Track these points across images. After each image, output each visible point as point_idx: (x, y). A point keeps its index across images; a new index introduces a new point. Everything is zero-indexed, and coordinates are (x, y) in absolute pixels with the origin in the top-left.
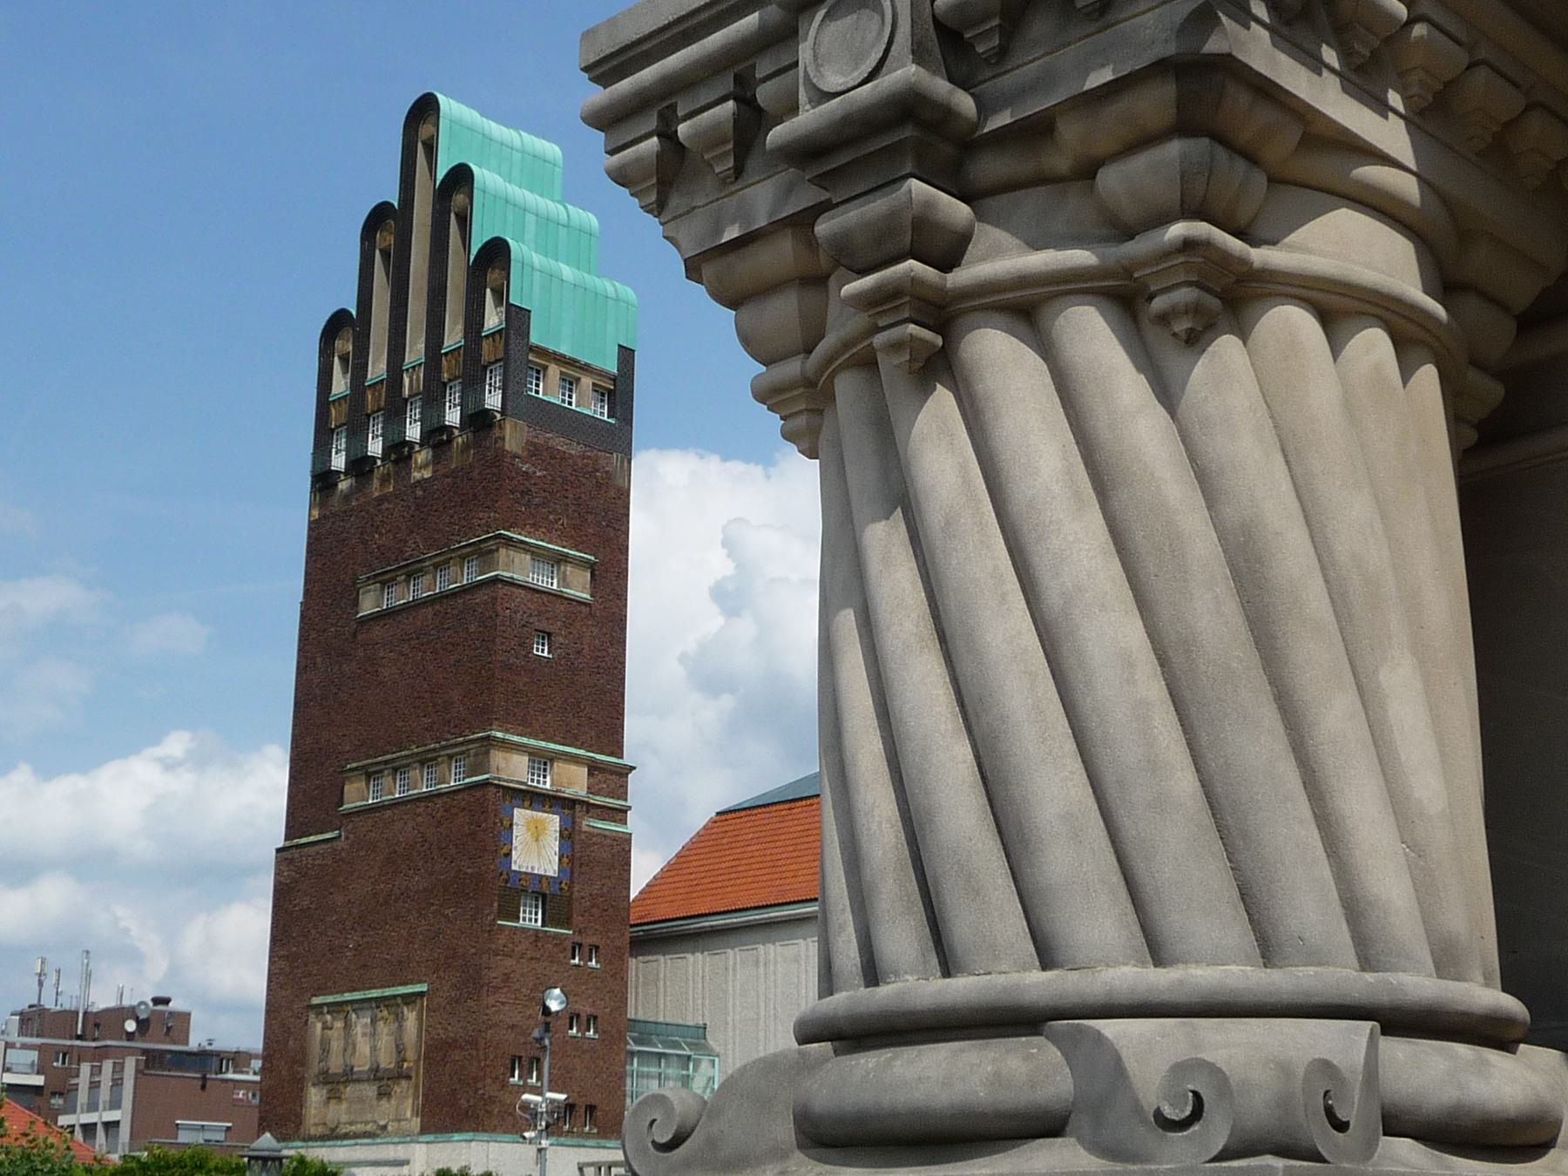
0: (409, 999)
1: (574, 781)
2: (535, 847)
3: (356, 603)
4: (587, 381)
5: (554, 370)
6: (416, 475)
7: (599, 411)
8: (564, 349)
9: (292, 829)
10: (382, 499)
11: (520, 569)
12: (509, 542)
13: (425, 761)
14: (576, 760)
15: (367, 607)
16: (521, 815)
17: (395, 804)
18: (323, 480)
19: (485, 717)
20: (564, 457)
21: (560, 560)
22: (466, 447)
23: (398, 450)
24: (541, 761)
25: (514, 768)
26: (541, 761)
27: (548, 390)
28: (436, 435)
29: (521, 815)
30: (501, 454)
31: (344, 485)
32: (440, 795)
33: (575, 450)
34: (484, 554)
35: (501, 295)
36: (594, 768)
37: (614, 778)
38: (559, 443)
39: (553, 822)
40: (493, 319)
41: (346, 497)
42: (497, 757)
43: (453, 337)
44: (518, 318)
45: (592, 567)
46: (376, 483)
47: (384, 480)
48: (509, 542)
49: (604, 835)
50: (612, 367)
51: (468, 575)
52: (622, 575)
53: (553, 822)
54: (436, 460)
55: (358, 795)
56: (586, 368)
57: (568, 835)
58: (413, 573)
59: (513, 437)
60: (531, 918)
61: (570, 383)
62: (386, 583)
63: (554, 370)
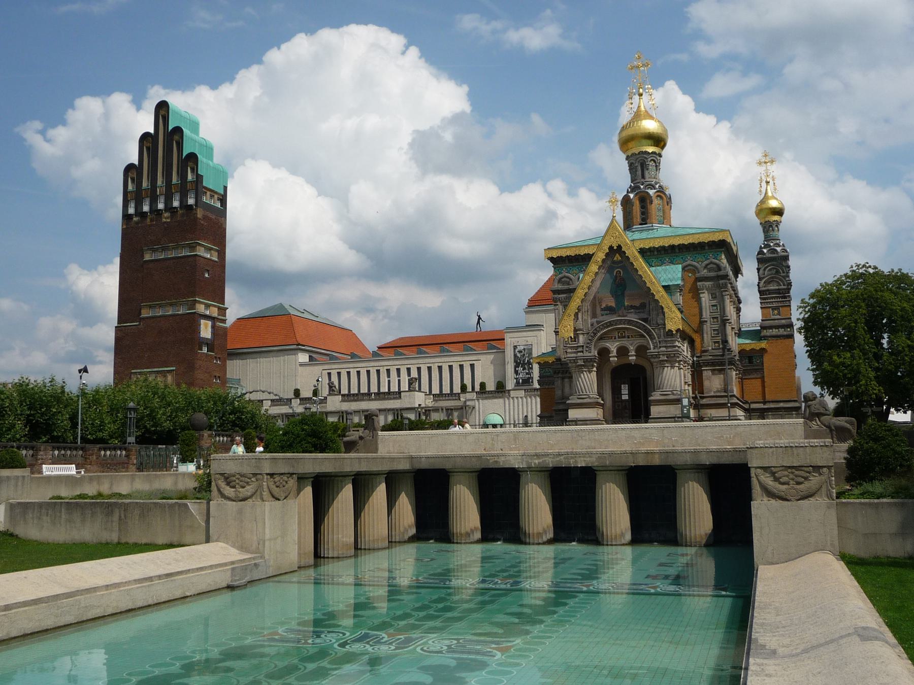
0: (169, 371)
1: (214, 312)
2: (206, 331)
3: (143, 256)
4: (216, 196)
5: (208, 193)
6: (164, 220)
7: (218, 205)
8: (211, 187)
9: (120, 319)
10: (151, 225)
11: (201, 252)
12: (200, 245)
13: (171, 305)
14: (215, 306)
15: (147, 257)
16: (203, 321)
17: (160, 317)
18: (126, 217)
19: (193, 294)
20: (211, 219)
21: (211, 249)
22: (183, 215)
23: (154, 211)
24: (207, 306)
25: (201, 308)
26: (207, 306)
27: (206, 199)
28: (169, 208)
29: (203, 321)
30: (196, 219)
31: (135, 219)
32: (178, 315)
33: (214, 217)
34: (192, 247)
35: (195, 170)
36: (219, 308)
37: (223, 311)
38: (210, 215)
39: (210, 323)
40: (190, 177)
41: (137, 223)
42: (197, 305)
43: (175, 180)
44: (199, 178)
45: (217, 251)
46: (148, 220)
47: (152, 220)
48: (200, 245)
49: (221, 327)
50: (222, 193)
51: (185, 253)
52: (225, 253)
53: (210, 323)
54: (172, 217)
55: (145, 313)
56: (216, 193)
57: (213, 327)
58: (164, 249)
59: (200, 213)
60: (205, 350)
61: (212, 196)
62: (154, 250)
63: (208, 193)
